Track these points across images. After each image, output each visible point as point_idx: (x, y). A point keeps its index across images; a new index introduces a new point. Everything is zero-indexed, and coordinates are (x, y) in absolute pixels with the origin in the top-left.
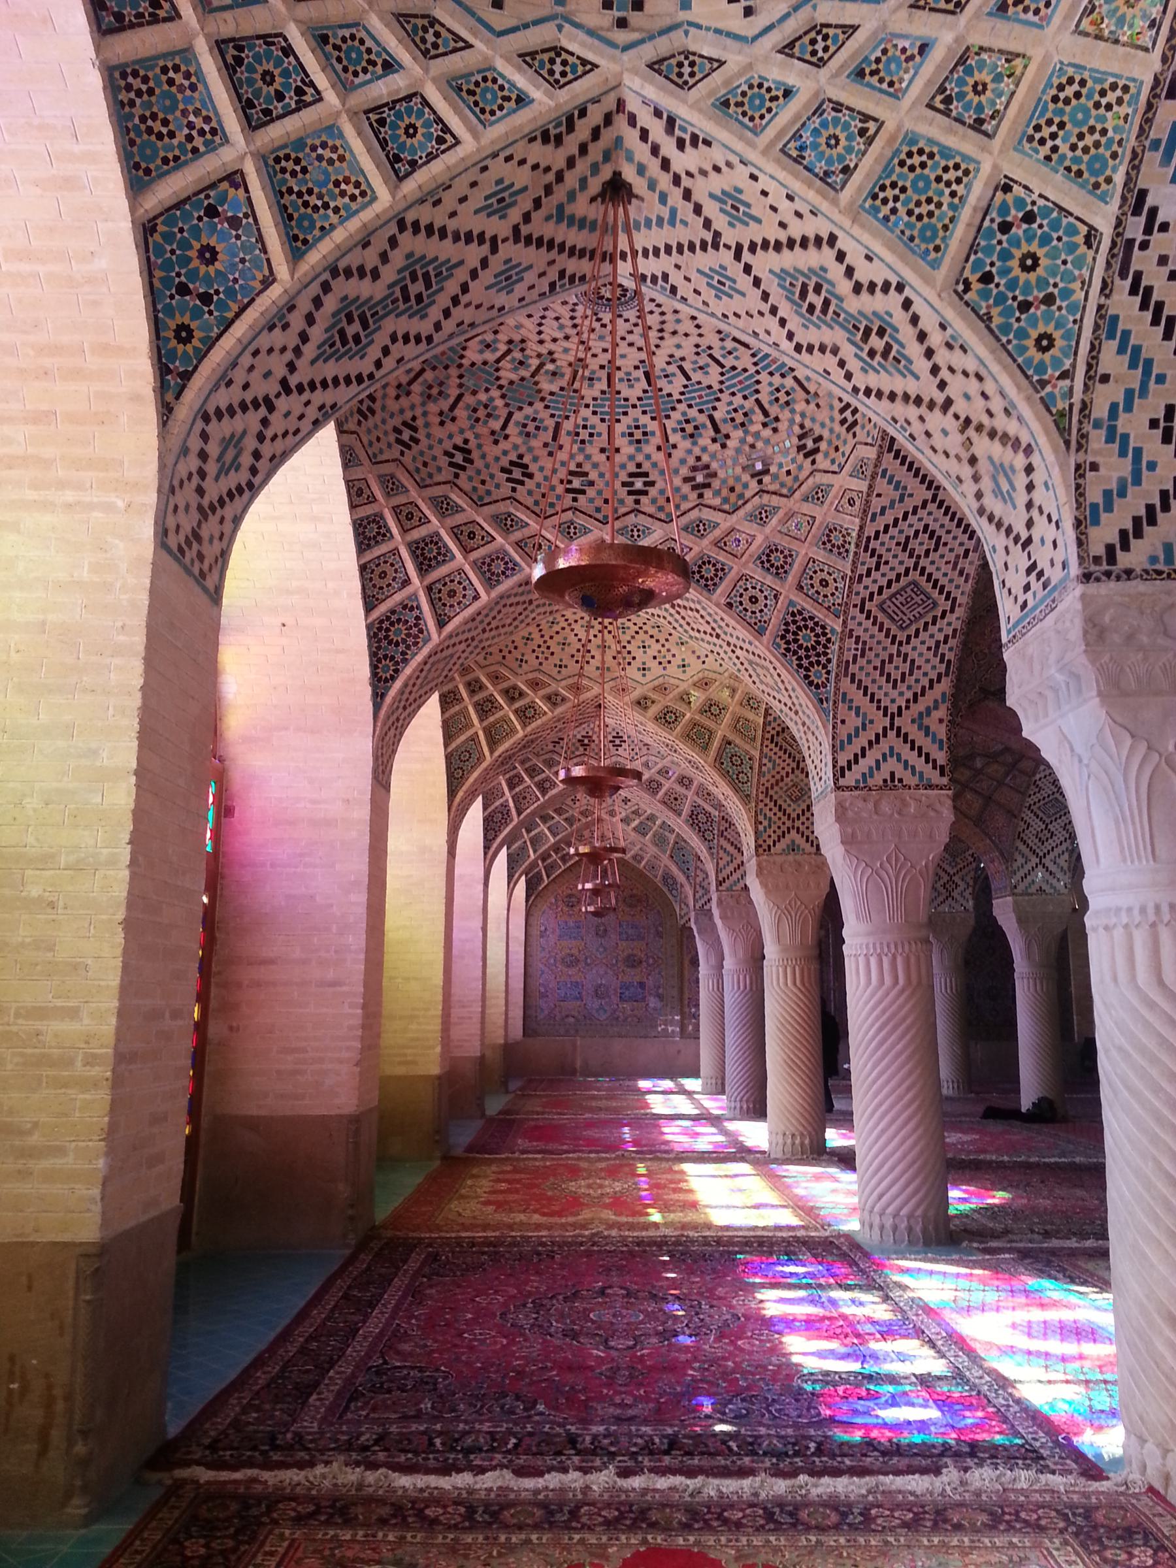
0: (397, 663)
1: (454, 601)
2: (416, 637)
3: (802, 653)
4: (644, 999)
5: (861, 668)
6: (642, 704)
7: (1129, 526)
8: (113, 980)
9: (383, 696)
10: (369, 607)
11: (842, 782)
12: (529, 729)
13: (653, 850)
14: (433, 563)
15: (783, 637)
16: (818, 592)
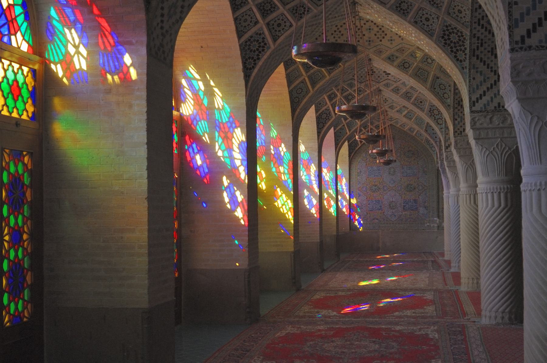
0: (255, 60)
1: (280, 28)
2: (263, 47)
3: (452, 45)
4: (417, 208)
5: (481, 52)
6: (390, 59)
7: (531, 27)
8: (146, 219)
9: (249, 76)
10: (239, 37)
11: (474, 109)
12: (332, 75)
13: (417, 128)
14: (269, 12)
15: (443, 37)
16: (457, 16)
